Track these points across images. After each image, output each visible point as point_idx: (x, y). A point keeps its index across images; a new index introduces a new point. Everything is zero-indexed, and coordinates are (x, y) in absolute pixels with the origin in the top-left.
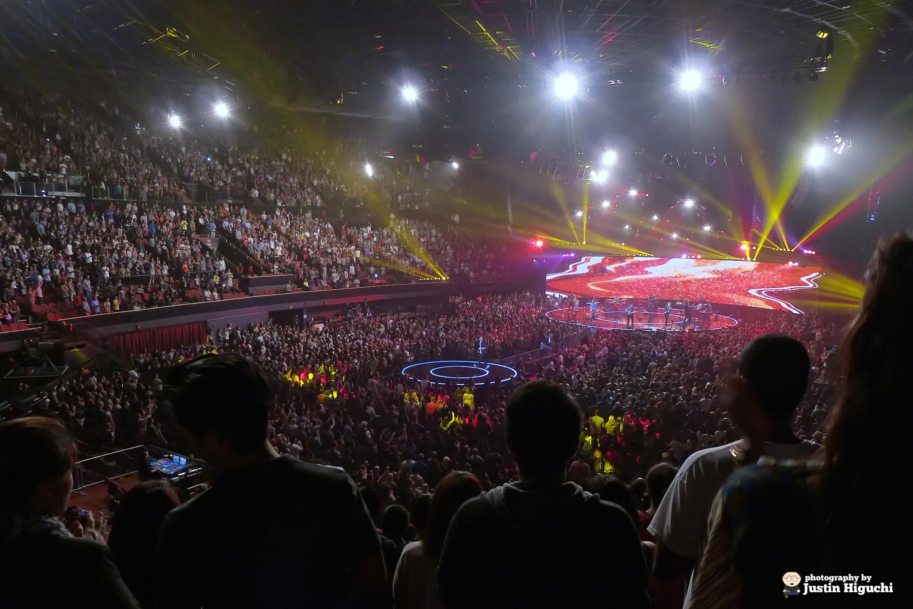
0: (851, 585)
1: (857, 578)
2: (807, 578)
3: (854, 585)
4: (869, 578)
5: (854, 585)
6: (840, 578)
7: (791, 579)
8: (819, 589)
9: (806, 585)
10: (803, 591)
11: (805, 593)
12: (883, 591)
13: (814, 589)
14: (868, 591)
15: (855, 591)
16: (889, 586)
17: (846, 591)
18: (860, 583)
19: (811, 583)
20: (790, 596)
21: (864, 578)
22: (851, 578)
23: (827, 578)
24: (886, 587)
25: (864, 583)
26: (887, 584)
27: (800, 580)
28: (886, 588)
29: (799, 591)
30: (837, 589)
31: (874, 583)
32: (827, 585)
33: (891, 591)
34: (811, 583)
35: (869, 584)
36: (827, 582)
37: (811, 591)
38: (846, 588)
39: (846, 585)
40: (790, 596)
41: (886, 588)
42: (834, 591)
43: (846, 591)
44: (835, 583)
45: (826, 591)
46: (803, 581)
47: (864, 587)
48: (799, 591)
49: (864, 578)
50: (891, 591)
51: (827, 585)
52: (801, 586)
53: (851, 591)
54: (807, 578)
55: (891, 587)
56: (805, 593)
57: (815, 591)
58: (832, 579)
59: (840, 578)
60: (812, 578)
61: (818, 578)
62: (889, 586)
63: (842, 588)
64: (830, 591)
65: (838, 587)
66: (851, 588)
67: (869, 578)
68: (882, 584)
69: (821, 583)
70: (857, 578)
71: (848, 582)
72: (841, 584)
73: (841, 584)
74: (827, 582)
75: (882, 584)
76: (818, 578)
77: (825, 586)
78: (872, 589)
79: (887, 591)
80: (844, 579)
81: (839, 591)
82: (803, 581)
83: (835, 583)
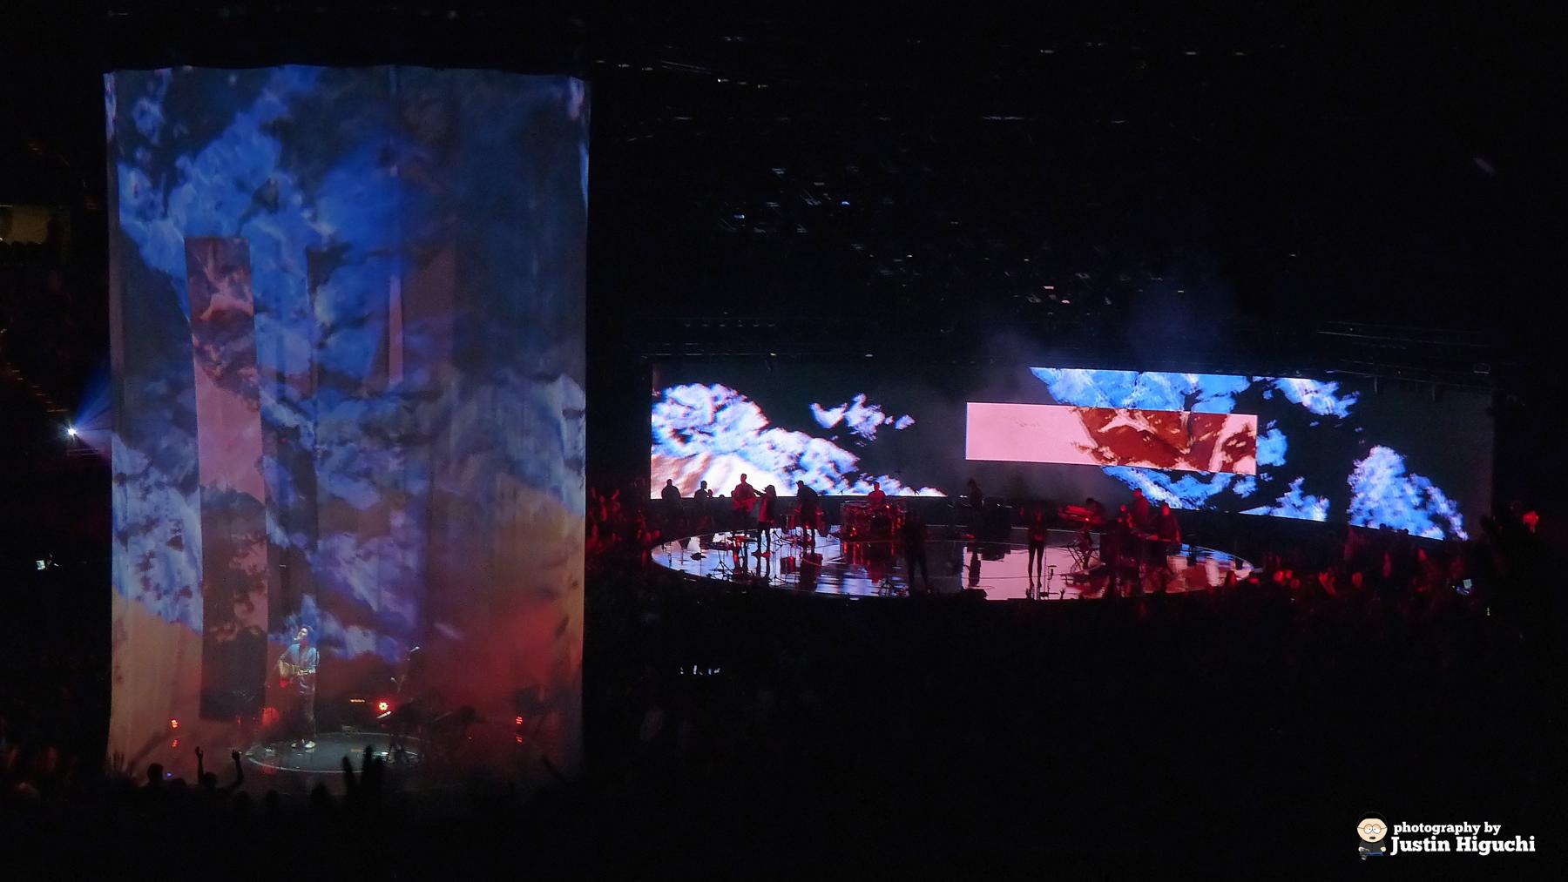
0: (1468, 839)
1: (1477, 828)
2: (1397, 829)
3: (1473, 840)
4: (1497, 828)
5: (1473, 840)
6: (1451, 829)
7: (1371, 830)
8: (1416, 846)
9: (1395, 839)
10: (1390, 848)
11: (1394, 853)
12: (1519, 849)
13: (1408, 847)
17: (1459, 849)
18: (1482, 836)
19: (1403, 836)
21: (1488, 828)
22: (1467, 827)
23: (1429, 828)
25: (1490, 837)
28: (1522, 845)
30: (1444, 846)
31: (1503, 836)
33: (1532, 849)
34: (1403, 836)
35: (1497, 838)
36: (1429, 835)
38: (1460, 844)
39: (1459, 839)
40: (1369, 857)
41: (1522, 845)
43: (1459, 849)
44: (1441, 837)
46: (1390, 833)
47: (1488, 843)
49: (1488, 828)
52: (1387, 841)
53: (1468, 849)
54: (1397, 829)
56: (1394, 853)
58: (1437, 829)
59: (1451, 829)
60: (1405, 828)
61: (1415, 829)
63: (1453, 844)
65: (1447, 843)
66: (1467, 844)
67: (1497, 828)
69: (1420, 836)
70: (1477, 828)
71: (1463, 834)
72: (1451, 838)
73: (1451, 838)
76: (1415, 829)
77: (1426, 841)
78: (1502, 846)
80: (1458, 829)
81: (1448, 849)
82: (1390, 833)
83: (1441, 837)
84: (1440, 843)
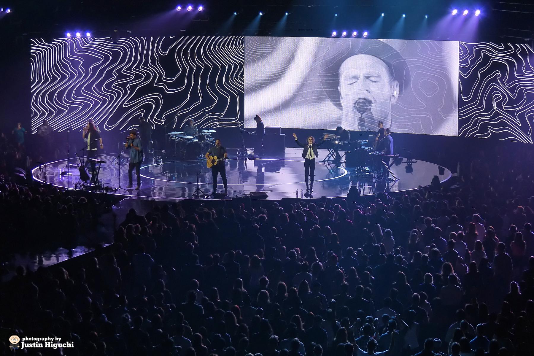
0: (49, 343)
1: (52, 339)
2: (24, 339)
3: (52, 343)
4: (60, 339)
5: (52, 343)
6: (43, 339)
7: (14, 339)
8: (30, 346)
9: (23, 343)
10: (21, 346)
12: (68, 347)
13: (28, 346)
14: (59, 346)
15: (52, 347)
17: (46, 347)
18: (54, 342)
19: (26, 342)
22: (49, 339)
23: (35, 339)
24: (70, 344)
26: (70, 342)
27: (19, 340)
28: (70, 345)
29: (19, 347)
30: (41, 345)
31: (62, 342)
33: (73, 347)
34: (26, 342)
35: (60, 342)
37: (26, 346)
38: (46, 345)
39: (46, 343)
41: (70, 345)
42: (39, 347)
43: (46, 347)
46: (21, 341)
47: (56, 344)
48: (19, 347)
49: (57, 339)
50: (73, 347)
52: (20, 344)
53: (49, 347)
54: (24, 339)
55: (73, 344)
57: (28, 346)
58: (38, 339)
59: (43, 339)
60: (26, 339)
61: (30, 339)
63: (44, 345)
64: (37, 346)
65: (42, 344)
66: (49, 345)
67: (60, 339)
68: (68, 342)
69: (32, 342)
70: (52, 339)
71: (47, 341)
72: (43, 343)
73: (43, 343)
75: (68, 342)
76: (30, 339)
77: (34, 344)
78: (61, 346)
79: (70, 347)
80: (45, 339)
81: (42, 347)
82: (21, 341)
83: (39, 342)
84: (39, 344)
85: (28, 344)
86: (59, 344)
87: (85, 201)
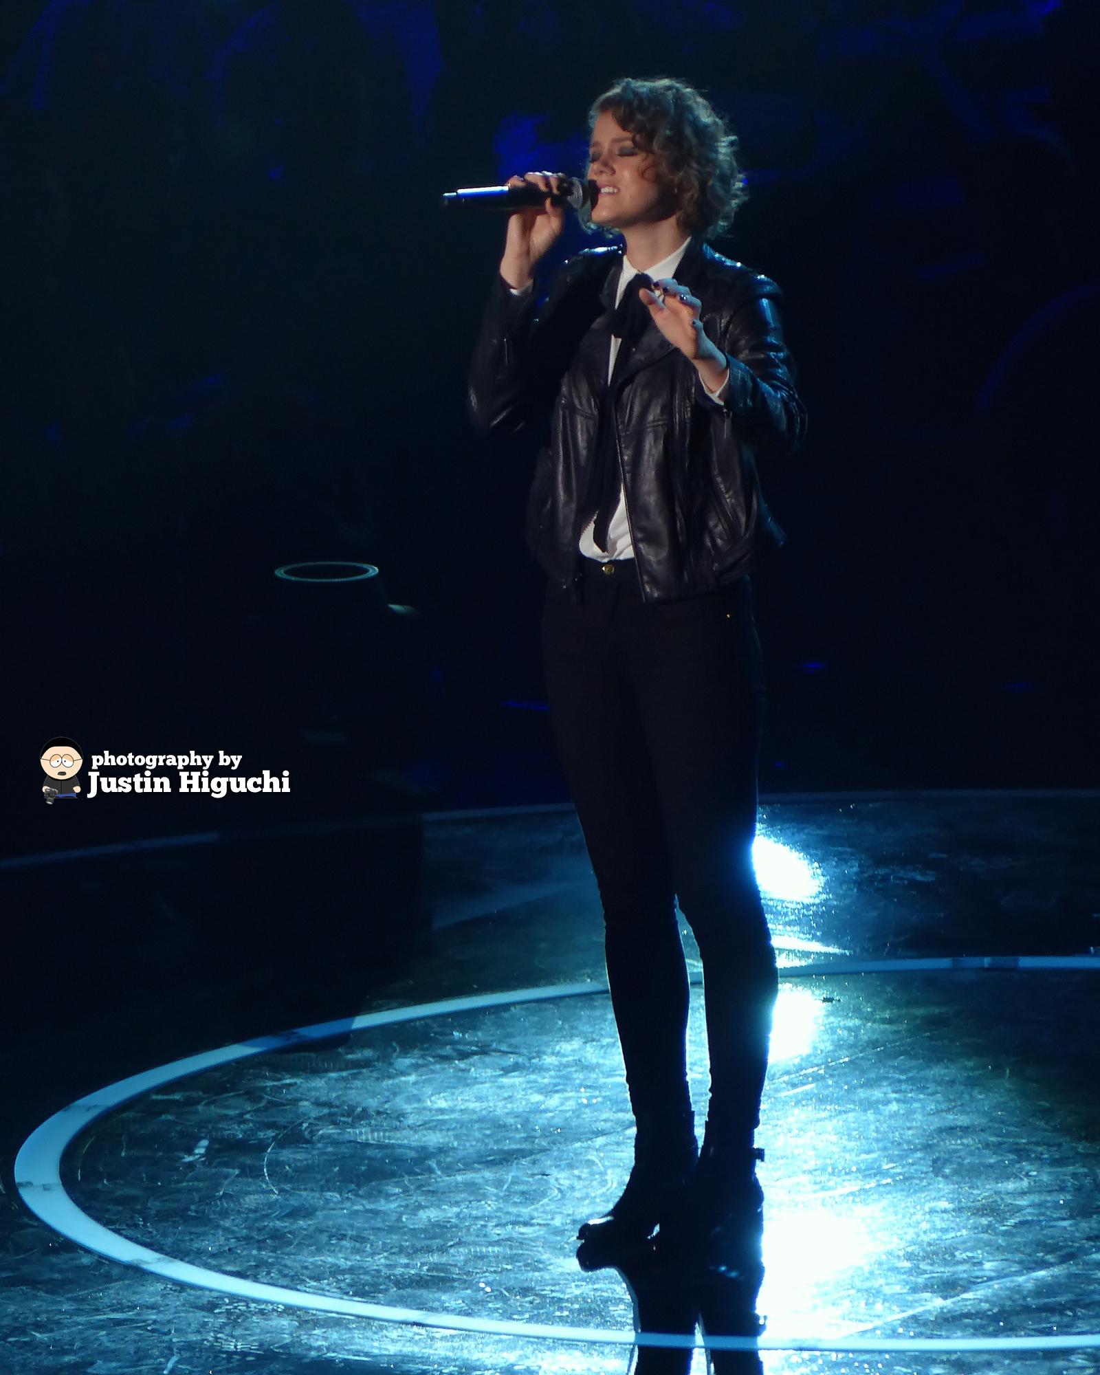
0: (196, 775)
1: (208, 760)
2: (97, 761)
3: (200, 776)
4: (237, 760)
5: (200, 776)
6: (172, 760)
7: (60, 762)
8: (123, 785)
9: (94, 776)
11: (93, 794)
12: (267, 789)
13: (111, 786)
14: (234, 789)
15: (205, 789)
16: (280, 777)
18: (217, 771)
19: (105, 771)
20: (57, 801)
21: (224, 760)
22: (194, 758)
23: (141, 760)
24: (275, 780)
25: (226, 772)
26: (276, 773)
27: (79, 764)
28: (273, 783)
29: (77, 789)
30: (163, 785)
31: (246, 770)
32: (143, 776)
33: (286, 789)
34: (105, 771)
36: (141, 770)
37: (105, 789)
38: (184, 782)
39: (184, 775)
40: (57, 801)
41: (273, 783)
42: (157, 789)
44: (159, 772)
45: (138, 790)
46: (87, 766)
47: (224, 781)
48: (77, 789)
49: (224, 760)
50: (286, 789)
51: (143, 776)
52: (82, 778)
53: (195, 789)
54: (97, 761)
55: (286, 781)
56: (93, 794)
57: (113, 789)
58: (152, 761)
59: (172, 760)
60: (108, 759)
61: (122, 760)
62: (280, 777)
63: (176, 783)
64: (148, 789)
65: (166, 781)
66: (195, 782)
67: (237, 760)
68: (266, 773)
69: (129, 771)
70: (208, 760)
71: (188, 768)
72: (172, 774)
73: (172, 774)
74: (141, 770)
75: (266, 773)
76: (122, 760)
77: (137, 779)
79: (277, 789)
81: (167, 789)
82: (87, 766)
83: (159, 772)
84: (157, 781)
85: (113, 780)
86: (233, 780)
87: (82, 1177)
